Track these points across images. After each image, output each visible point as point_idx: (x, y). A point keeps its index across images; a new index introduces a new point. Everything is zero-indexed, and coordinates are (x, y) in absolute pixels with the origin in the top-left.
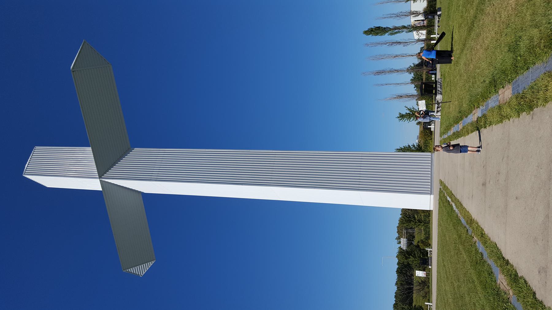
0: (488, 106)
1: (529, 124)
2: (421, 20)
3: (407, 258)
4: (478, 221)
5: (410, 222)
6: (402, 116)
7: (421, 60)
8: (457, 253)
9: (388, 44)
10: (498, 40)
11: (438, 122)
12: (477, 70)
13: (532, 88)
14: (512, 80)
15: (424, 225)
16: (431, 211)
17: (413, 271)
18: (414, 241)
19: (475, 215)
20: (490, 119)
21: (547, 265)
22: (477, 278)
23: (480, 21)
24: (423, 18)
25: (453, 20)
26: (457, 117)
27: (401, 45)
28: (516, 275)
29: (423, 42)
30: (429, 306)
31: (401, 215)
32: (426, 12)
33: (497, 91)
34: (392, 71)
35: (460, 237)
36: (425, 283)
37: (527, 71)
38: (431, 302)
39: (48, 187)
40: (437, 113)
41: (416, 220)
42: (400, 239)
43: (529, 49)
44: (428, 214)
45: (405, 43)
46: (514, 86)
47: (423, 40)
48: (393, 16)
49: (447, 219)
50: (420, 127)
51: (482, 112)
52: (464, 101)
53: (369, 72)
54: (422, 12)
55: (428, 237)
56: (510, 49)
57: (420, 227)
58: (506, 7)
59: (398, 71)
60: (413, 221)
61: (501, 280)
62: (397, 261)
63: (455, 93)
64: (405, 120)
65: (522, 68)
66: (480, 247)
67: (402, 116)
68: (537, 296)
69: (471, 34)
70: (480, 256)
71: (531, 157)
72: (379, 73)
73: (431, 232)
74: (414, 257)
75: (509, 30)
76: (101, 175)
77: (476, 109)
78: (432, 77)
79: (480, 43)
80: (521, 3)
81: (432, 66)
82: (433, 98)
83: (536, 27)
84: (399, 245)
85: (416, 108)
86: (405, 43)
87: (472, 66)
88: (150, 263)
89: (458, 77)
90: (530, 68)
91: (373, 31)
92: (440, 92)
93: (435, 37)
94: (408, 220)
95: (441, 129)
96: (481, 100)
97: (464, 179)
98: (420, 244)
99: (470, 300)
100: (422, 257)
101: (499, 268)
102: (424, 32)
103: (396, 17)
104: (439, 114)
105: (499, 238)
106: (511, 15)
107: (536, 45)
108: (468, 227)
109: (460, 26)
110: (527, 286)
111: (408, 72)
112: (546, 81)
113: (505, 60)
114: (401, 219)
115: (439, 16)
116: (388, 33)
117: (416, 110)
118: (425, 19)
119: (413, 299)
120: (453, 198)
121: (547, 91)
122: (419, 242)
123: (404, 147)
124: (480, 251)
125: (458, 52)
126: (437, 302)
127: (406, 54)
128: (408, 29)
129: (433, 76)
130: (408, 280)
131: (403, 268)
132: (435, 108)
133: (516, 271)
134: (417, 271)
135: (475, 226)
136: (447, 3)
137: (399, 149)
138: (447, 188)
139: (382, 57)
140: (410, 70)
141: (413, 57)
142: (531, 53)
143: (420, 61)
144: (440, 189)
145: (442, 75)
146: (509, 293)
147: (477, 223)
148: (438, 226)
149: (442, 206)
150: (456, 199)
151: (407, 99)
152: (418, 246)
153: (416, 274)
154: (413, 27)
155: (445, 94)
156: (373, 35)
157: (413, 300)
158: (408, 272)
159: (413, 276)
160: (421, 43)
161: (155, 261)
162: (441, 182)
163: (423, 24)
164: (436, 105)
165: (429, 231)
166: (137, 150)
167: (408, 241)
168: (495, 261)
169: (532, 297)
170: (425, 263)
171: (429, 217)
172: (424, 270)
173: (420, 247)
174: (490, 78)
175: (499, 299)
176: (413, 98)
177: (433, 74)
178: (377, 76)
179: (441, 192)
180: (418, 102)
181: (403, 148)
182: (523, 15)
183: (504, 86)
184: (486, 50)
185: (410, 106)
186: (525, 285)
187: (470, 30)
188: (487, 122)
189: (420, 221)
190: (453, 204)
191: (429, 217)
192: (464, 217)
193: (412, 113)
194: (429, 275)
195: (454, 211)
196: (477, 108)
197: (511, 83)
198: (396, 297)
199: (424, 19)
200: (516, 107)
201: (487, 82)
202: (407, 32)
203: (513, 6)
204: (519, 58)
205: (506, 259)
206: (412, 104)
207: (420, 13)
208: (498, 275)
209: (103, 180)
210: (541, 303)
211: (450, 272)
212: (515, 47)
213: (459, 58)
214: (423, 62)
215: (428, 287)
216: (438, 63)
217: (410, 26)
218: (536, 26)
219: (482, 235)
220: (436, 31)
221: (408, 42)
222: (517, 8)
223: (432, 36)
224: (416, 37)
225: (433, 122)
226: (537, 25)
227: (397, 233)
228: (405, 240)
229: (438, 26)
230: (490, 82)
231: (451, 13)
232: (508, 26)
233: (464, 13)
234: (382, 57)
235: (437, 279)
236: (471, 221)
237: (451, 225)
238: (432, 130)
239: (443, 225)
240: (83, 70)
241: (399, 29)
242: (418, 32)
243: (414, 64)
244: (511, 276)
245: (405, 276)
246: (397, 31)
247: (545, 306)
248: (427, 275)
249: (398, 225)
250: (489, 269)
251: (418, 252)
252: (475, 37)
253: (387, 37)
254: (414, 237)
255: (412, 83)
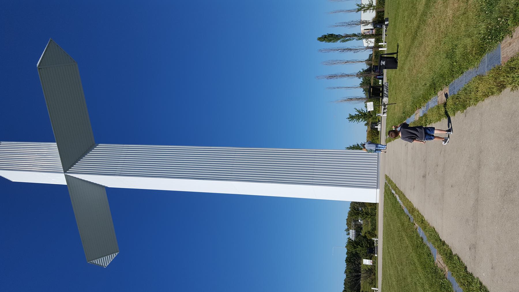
0: (429, 107)
1: (463, 121)
2: (370, 29)
3: (355, 248)
4: (419, 210)
5: (358, 215)
6: (352, 117)
7: (369, 66)
8: (400, 240)
9: (340, 51)
10: (438, 48)
11: (384, 122)
12: (419, 75)
13: (466, 89)
14: (449, 83)
15: (370, 217)
16: (377, 204)
17: (361, 260)
18: (361, 232)
19: (416, 204)
20: (430, 117)
21: (476, 242)
22: (418, 260)
23: (422, 30)
24: (372, 28)
25: (399, 29)
26: (402, 117)
27: (351, 52)
28: (451, 253)
29: (371, 50)
30: (375, 291)
31: (350, 208)
32: (375, 21)
33: (437, 93)
34: (343, 76)
35: (403, 225)
36: (372, 271)
37: (461, 75)
38: (377, 287)
39: (13, 181)
40: (383, 114)
41: (364, 213)
42: (349, 230)
43: (463, 56)
44: (374, 207)
45: (356, 50)
46: (451, 88)
47: (372, 47)
48: (345, 24)
49: (392, 210)
50: (368, 128)
51: (423, 112)
52: (407, 102)
53: (323, 76)
54: (371, 21)
55: (374, 228)
56: (447, 56)
57: (367, 219)
58: (445, 19)
59: (349, 76)
60: (361, 214)
61: (438, 259)
62: (346, 251)
63: (399, 95)
64: (355, 121)
65: (457, 72)
66: (421, 232)
67: (352, 117)
68: (468, 270)
69: (414, 43)
70: (421, 241)
71: (464, 150)
72: (332, 77)
73: (377, 224)
74: (362, 247)
75: (447, 39)
76: (66, 169)
77: (418, 110)
78: (379, 82)
79: (423, 50)
80: (457, 16)
81: (380, 71)
82: (380, 101)
83: (469, 37)
84: (348, 236)
85: (365, 110)
86: (356, 50)
87: (415, 71)
88: (113, 255)
89: (402, 81)
90: (464, 72)
91: (326, 38)
92: (387, 95)
93: (383, 45)
94: (356, 213)
95: (386, 129)
96: (423, 101)
97: (407, 172)
98: (367, 235)
99: (412, 281)
100: (369, 246)
101: (436, 249)
102: (373, 40)
103: (348, 26)
104: (385, 115)
105: (436, 223)
106: (449, 26)
107: (469, 52)
108: (410, 215)
109: (405, 35)
110: (460, 262)
111: (357, 76)
112: (477, 83)
113: (444, 65)
114: (350, 211)
115: (387, 25)
116: (340, 41)
117: (364, 111)
118: (374, 28)
119: (361, 285)
120: (397, 191)
121: (478, 92)
122: (366, 233)
123: (353, 145)
124: (420, 236)
125: (403, 58)
126: (382, 286)
127: (356, 60)
128: (359, 37)
129: (380, 81)
130: (356, 268)
131: (351, 257)
132: (381, 110)
133: (451, 250)
134: (364, 260)
135: (416, 213)
136: (394, 14)
137: (349, 148)
138: (392, 181)
139: (334, 62)
140: (359, 75)
141: (362, 63)
142: (465, 59)
143: (368, 67)
144: (386, 183)
145: (388, 80)
146: (445, 270)
147: (418, 211)
148: (384, 217)
149: (388, 199)
150: (399, 191)
151: (356, 102)
152: (365, 237)
153: (363, 262)
154: (363, 35)
155: (390, 97)
156: (326, 42)
157: (360, 286)
158: (356, 261)
159: (361, 265)
160: (370, 50)
161: (118, 253)
162: (387, 177)
163: (371, 33)
164: (383, 107)
165: (375, 223)
166: (101, 146)
167: (356, 232)
168: (434, 243)
169: (464, 271)
170: (371, 252)
171: (375, 209)
172: (370, 259)
173: (367, 237)
174: (430, 81)
175: (437, 276)
176: (362, 101)
177: (380, 79)
178: (329, 80)
179: (386, 185)
180: (366, 105)
181: (353, 146)
182: (459, 26)
183: (442, 88)
184: (427, 56)
185: (359, 108)
186: (458, 261)
187: (414, 38)
188: (427, 121)
189: (367, 214)
190: (397, 196)
191: (375, 210)
192: (407, 207)
193: (361, 114)
194: (375, 263)
195: (398, 202)
196: (419, 108)
197: (448, 85)
198: (345, 284)
199: (373, 28)
200: (452, 107)
201: (428, 85)
202: (357, 40)
203: (450, 18)
204: (455, 64)
205: (443, 240)
206: (361, 106)
207: (369, 23)
208: (436, 256)
209: (68, 174)
210: (471, 275)
211: (394, 258)
212: (452, 54)
213: (404, 64)
214: (371, 68)
215: (375, 274)
216: (385, 69)
217: (360, 34)
218: (469, 36)
219: (423, 221)
220: (384, 39)
221: (358, 49)
222: (454, 20)
223: (380, 44)
224: (366, 45)
225: (379, 123)
226: (470, 35)
227: (347, 225)
228: (353, 231)
229: (385, 35)
230: (430, 85)
231: (397, 23)
232: (446, 35)
233: (409, 23)
234: (334, 62)
235: (383, 265)
236: (413, 210)
237: (395, 215)
238: (379, 130)
239: (388, 216)
240: (54, 67)
241: (350, 37)
242: (367, 40)
243: (363, 69)
244: (446, 255)
245: (354, 264)
246: (348, 38)
247: (474, 277)
248: (374, 263)
249: (347, 218)
250: (428, 251)
251: (365, 242)
252: (418, 45)
253: (339, 44)
254: (361, 229)
255: (361, 87)
